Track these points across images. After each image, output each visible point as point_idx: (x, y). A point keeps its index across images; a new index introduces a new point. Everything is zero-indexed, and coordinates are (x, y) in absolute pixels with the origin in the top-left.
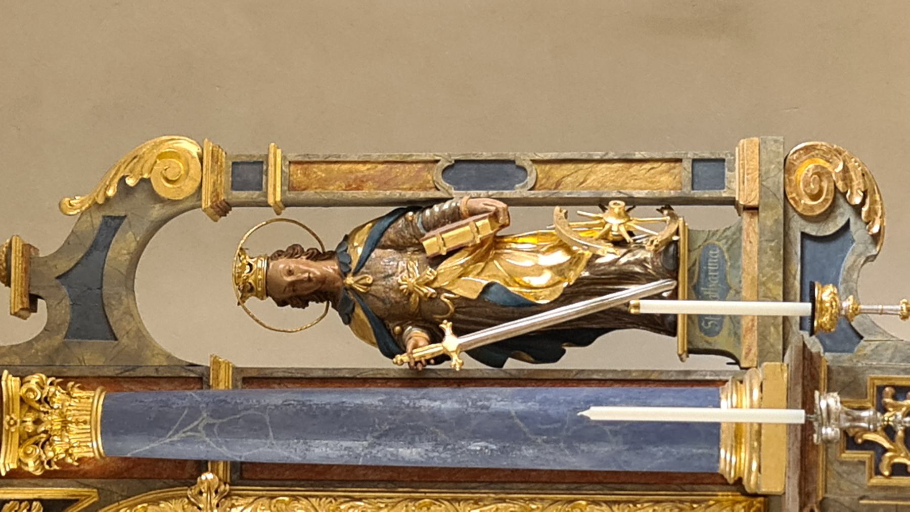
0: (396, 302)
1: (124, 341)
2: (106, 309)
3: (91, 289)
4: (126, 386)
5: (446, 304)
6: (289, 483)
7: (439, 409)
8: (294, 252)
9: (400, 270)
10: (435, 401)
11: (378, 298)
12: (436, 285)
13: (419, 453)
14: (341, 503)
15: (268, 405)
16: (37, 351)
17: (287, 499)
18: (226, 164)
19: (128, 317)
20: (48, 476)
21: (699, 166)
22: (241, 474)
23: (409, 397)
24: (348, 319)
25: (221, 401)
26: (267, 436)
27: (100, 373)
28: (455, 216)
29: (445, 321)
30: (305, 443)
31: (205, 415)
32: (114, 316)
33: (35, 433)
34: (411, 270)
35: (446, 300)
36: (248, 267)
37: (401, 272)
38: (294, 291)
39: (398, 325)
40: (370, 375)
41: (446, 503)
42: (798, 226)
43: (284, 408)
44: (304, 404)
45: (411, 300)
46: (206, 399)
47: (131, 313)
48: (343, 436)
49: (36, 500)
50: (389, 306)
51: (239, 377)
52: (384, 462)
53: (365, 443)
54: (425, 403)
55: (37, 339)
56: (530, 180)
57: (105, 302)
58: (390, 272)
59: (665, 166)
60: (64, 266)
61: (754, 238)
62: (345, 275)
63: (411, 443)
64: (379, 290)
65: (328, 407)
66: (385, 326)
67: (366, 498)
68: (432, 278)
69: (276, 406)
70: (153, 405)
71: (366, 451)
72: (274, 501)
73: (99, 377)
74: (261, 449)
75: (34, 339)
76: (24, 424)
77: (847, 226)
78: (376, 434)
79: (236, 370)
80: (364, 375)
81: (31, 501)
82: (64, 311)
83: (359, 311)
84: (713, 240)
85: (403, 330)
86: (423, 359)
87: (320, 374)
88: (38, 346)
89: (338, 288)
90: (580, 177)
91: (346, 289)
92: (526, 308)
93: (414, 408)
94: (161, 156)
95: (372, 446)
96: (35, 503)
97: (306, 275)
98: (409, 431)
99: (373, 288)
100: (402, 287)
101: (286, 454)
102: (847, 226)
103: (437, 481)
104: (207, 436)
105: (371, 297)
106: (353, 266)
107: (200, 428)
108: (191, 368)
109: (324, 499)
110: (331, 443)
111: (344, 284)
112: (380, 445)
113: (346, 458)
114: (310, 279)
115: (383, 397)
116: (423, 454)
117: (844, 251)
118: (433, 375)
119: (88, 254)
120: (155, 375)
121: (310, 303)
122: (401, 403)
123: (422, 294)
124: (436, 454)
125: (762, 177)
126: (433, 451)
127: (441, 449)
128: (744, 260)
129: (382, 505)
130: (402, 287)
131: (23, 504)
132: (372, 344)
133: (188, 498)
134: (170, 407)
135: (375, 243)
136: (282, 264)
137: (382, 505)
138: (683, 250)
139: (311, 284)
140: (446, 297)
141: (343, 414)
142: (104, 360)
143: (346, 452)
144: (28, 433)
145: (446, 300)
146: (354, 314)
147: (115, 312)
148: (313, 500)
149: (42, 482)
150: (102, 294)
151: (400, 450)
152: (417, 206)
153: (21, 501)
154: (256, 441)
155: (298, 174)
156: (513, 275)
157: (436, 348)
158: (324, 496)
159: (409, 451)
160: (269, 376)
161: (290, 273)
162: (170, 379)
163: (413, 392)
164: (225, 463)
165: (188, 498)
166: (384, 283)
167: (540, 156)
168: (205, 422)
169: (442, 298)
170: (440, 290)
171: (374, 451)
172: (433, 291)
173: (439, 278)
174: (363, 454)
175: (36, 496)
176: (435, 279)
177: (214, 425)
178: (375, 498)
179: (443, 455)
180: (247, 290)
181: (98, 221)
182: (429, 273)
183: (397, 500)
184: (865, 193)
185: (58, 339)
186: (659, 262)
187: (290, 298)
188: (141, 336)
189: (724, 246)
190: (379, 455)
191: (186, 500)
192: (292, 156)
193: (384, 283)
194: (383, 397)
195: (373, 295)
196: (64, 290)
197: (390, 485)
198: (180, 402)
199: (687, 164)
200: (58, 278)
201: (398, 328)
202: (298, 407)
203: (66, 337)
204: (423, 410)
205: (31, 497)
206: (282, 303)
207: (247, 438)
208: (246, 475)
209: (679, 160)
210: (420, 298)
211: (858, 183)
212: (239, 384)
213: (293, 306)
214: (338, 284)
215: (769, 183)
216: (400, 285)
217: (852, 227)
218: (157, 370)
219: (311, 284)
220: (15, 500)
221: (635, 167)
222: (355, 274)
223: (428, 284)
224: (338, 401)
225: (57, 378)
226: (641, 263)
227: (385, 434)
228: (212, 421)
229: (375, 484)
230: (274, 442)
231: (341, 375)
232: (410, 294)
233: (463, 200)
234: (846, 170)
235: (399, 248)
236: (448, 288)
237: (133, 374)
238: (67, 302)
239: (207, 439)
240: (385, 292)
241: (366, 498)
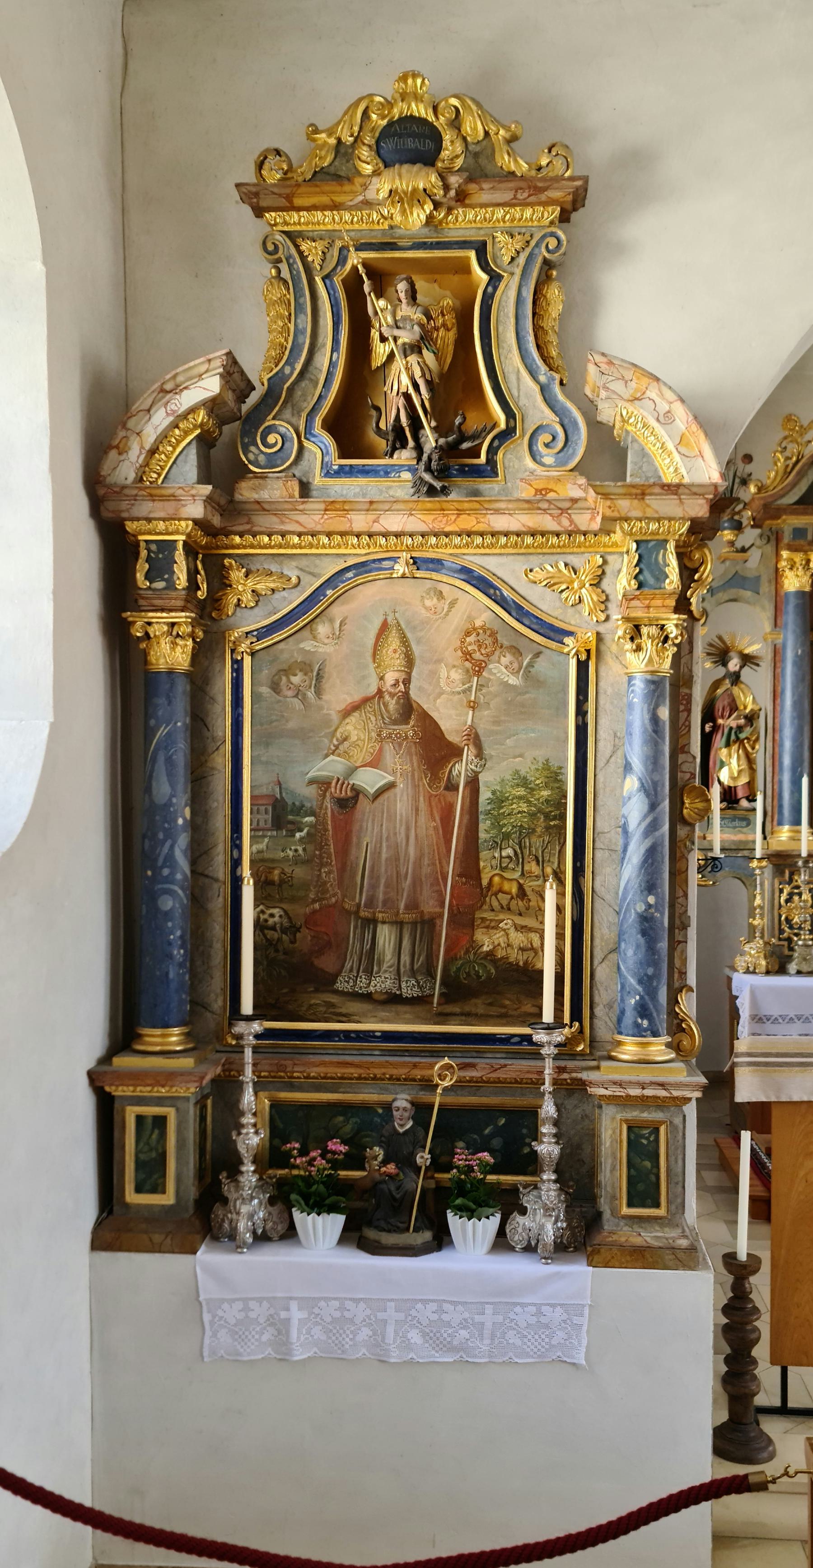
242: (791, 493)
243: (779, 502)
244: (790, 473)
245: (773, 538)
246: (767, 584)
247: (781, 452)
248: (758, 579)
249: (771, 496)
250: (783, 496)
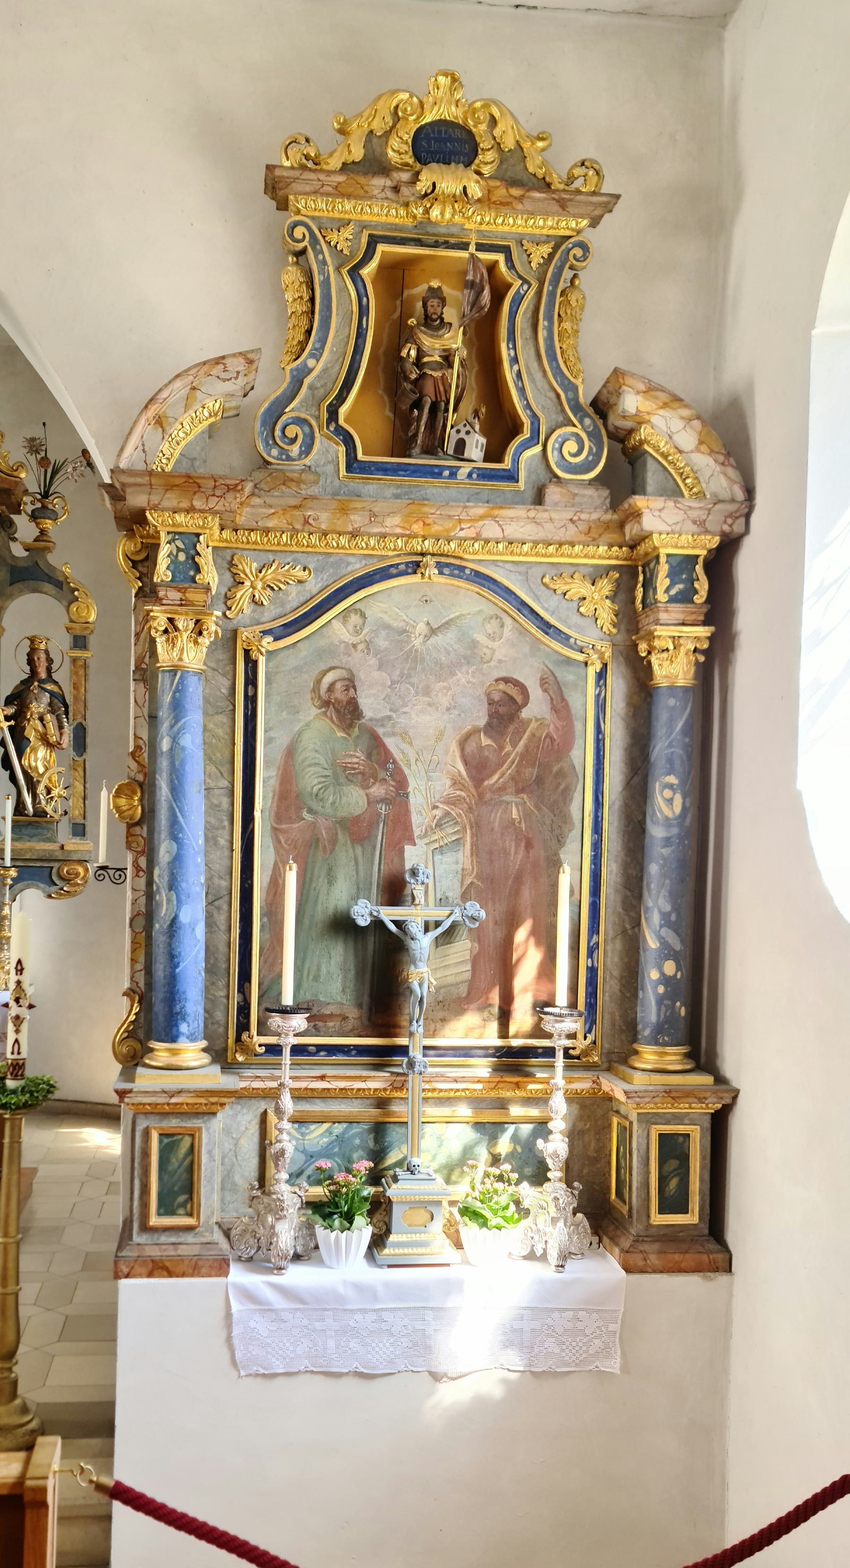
1: (10, 589)
8: (50, 661)
18: (86, 633)
21: (82, 827)
24: (22, 682)
28: (61, 727)
32: (20, 585)
42: (56, 865)
47: (21, 592)
56: (77, 758)
59: (82, 812)
60: (41, 564)
61: (51, 848)
62: (39, 681)
77: (56, 885)
82: (22, 564)
84: (51, 832)
90: (79, 779)
92: (20, 756)
94: (88, 606)
102: (56, 885)
106: (43, 685)
117: (45, 883)
119: (47, 575)
125: (76, 851)
128: (42, 844)
135: (52, 694)
136: (43, 656)
138: (45, 819)
152: (67, 713)
155: (80, 663)
156: (34, 750)
161: (39, 659)
167: (87, 763)
180: (32, 640)
181: (61, 579)
182: (36, 716)
184: (68, 892)
185: (10, 561)
186: (40, 810)
189: (49, 835)
192: (88, 661)
196: (31, 564)
199: (82, 822)
206: (28, 655)
209: (84, 818)
211: (72, 889)
215: (73, 854)
217: (55, 887)
221: (81, 801)
226: (40, 803)
233: (68, 730)
234: (78, 885)
235: (50, 704)
238: (26, 565)
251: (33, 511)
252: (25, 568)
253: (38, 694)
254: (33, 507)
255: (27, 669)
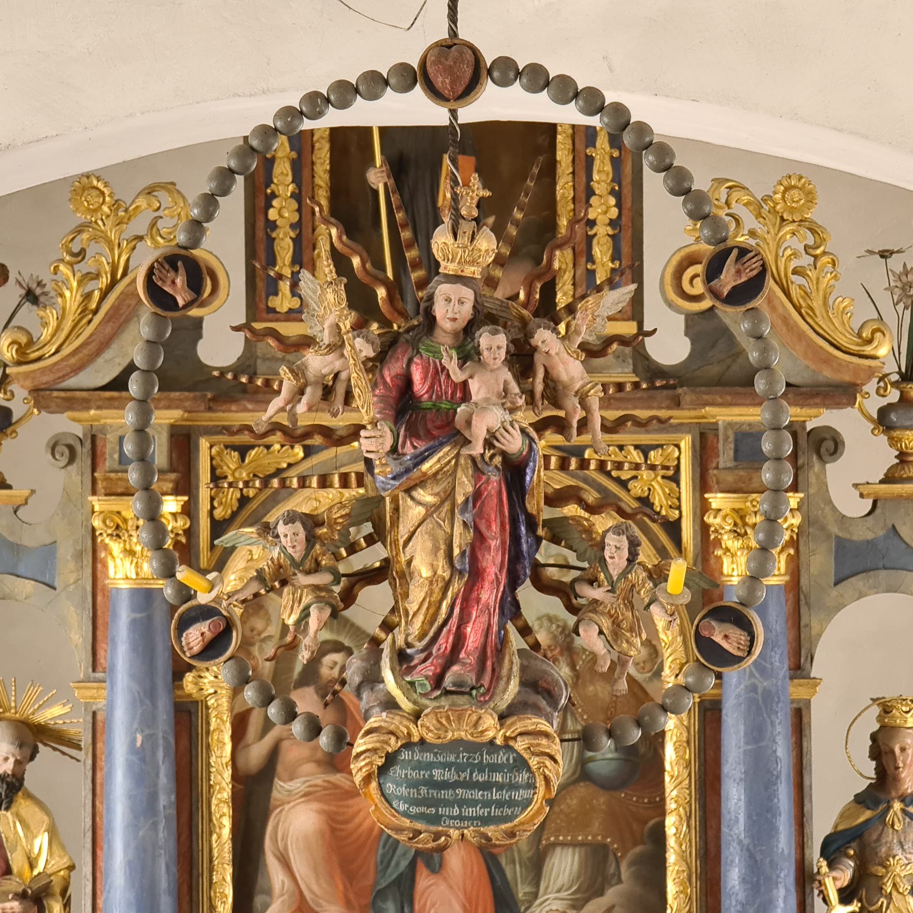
0: (877, 853)
1: (834, 592)
2: (864, 574)
3: (883, 558)
4: (791, 595)
5: (877, 902)
6: (702, 756)
7: (776, 907)
9: (908, 856)
10: (785, 902)
11: (880, 835)
12: (895, 894)
13: (734, 887)
14: (684, 809)
15: (776, 743)
16: (823, 510)
17: (687, 757)
19: (857, 595)
20: (704, 528)
22: (709, 709)
23: (787, 876)
25: (779, 698)
26: (747, 743)
27: (803, 572)
29: (859, 905)
30: (741, 780)
31: (765, 684)
32: (857, 582)
33: (745, 524)
34: (908, 867)
35: (880, 903)
36: (908, 709)
37: (906, 858)
38: (886, 753)
39: (855, 851)
40: (807, 830)
41: (687, 908)
43: (773, 759)
44: (778, 777)
45: (880, 868)
46: (780, 683)
48: (749, 816)
49: (681, 512)
50: (873, 845)
51: (801, 705)
52: (724, 854)
53: (743, 835)
54: (782, 892)
55: (834, 509)
57: (872, 573)
58: (906, 847)
62: (902, 799)
63: (744, 881)
64: (888, 836)
65: (776, 800)
66: (853, 840)
67: (689, 831)
68: (901, 890)
69: (775, 752)
70: (774, 632)
71: (735, 837)
72: (685, 745)
73: (799, 570)
74: (734, 736)
75: (834, 506)
76: (753, 515)
78: (751, 847)
79: (808, 703)
80: (806, 824)
81: (679, 508)
82: (862, 534)
83: (868, 814)
85: (850, 857)
86: (823, 888)
87: (806, 782)
88: (827, 509)
89: (890, 793)
91: (889, 802)
93: (777, 883)
95: (740, 842)
96: (677, 512)
97: (901, 765)
98: (755, 879)
99: (891, 830)
100: (891, 859)
101: (730, 760)
103: (706, 895)
104: (746, 687)
105: (881, 828)
107: (753, 680)
108: (809, 659)
109: (688, 792)
110: (742, 804)
111: (893, 799)
112: (741, 850)
113: (728, 817)
114: (897, 768)
115: (786, 852)
116: (734, 890)
118: (808, 891)
120: (802, 624)
121: (874, 763)
122: (782, 870)
123: (886, 880)
124: (734, 903)
126: (737, 901)
127: (739, 908)
129: (683, 847)
130: (891, 859)
131: (676, 501)
132: (836, 826)
133: (686, 663)
134: (772, 650)
137: (683, 847)
139: (892, 768)
140: (882, 903)
141: (769, 816)
142: (816, 573)
143: (733, 817)
144: (745, 516)
145: (880, 903)
146: (864, 809)
147: (861, 583)
148: (687, 782)
149: (698, 521)
150: (878, 569)
151: (737, 870)
153: (679, 499)
154: (742, 733)
157: (833, 896)
158: (691, 792)
159: (736, 878)
160: (804, 734)
162: (798, 638)
163: (791, 880)
164: (720, 695)
165: (686, 663)
166: (895, 841)
168: (759, 684)
169: (882, 899)
170: (889, 897)
171: (735, 844)
172: (888, 891)
173: (900, 896)
174: (732, 833)
175: (684, 513)
176: (899, 893)
177: (757, 694)
178: (690, 841)
179: (732, 909)
180: (886, 709)
183: (689, 861)
185: (834, 530)
187: (879, 746)
188: (838, 608)
190: (732, 849)
191: (684, 661)
193: (895, 841)
194: (786, 852)
195: (883, 830)
196: (881, 533)
197: (703, 851)
198: (777, 659)
200: (893, 526)
201: (852, 852)
202: (775, 773)
203: (837, 537)
204: (775, 891)
205: (684, 508)
206: (874, 737)
207: (745, 724)
208: (708, 714)
210: (882, 877)
212: (795, 705)
213: (871, 746)
214: (894, 794)
216: (894, 857)
218: (807, 626)
219: (892, 768)
220: (680, 493)
222: (903, 811)
223: (894, 885)
224: (782, 810)
225: (797, 534)
227: (752, 856)
228: (760, 690)
229: (703, 837)
230: (742, 750)
231: (806, 801)
232: (885, 867)
236: (891, 906)
237: (803, 602)
238: (870, 536)
239: (742, 686)
240: (886, 843)
241: (689, 831)
242: (100, 360)
243: (71, 382)
244: (95, 312)
245: (83, 453)
246: (72, 565)
247: (71, 264)
248: (51, 548)
249: (50, 368)
250: (77, 369)
251: (883, 412)
252: (870, 544)
253: (904, 831)
254: (884, 402)
255: (870, 769)
